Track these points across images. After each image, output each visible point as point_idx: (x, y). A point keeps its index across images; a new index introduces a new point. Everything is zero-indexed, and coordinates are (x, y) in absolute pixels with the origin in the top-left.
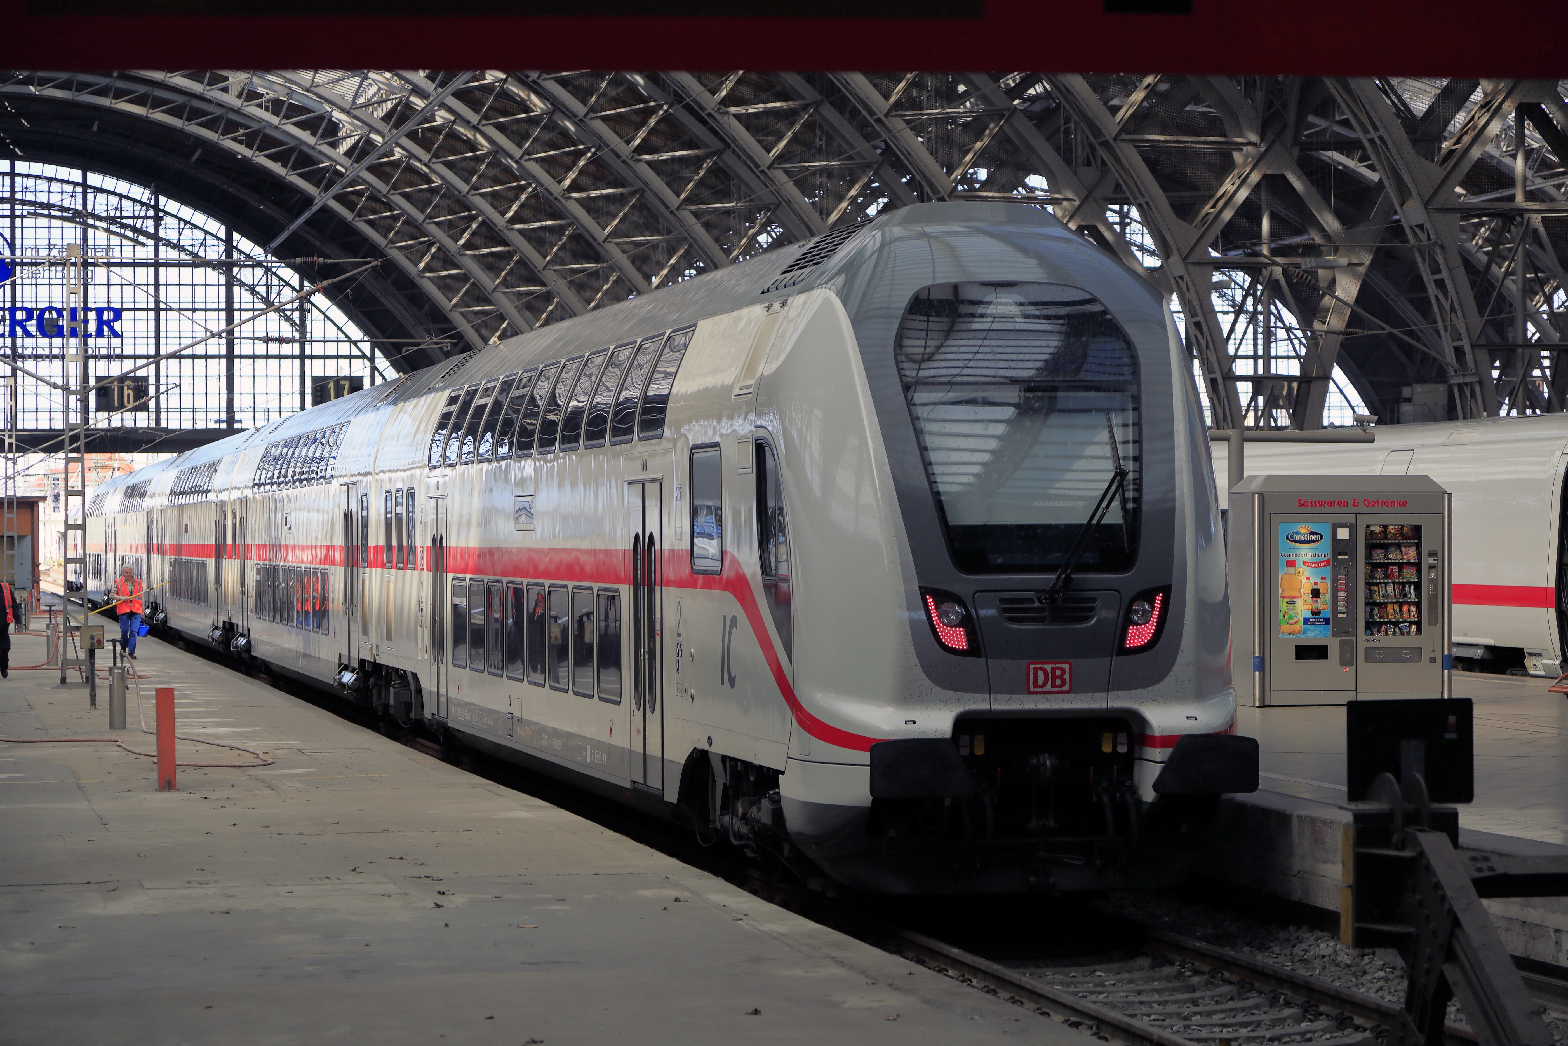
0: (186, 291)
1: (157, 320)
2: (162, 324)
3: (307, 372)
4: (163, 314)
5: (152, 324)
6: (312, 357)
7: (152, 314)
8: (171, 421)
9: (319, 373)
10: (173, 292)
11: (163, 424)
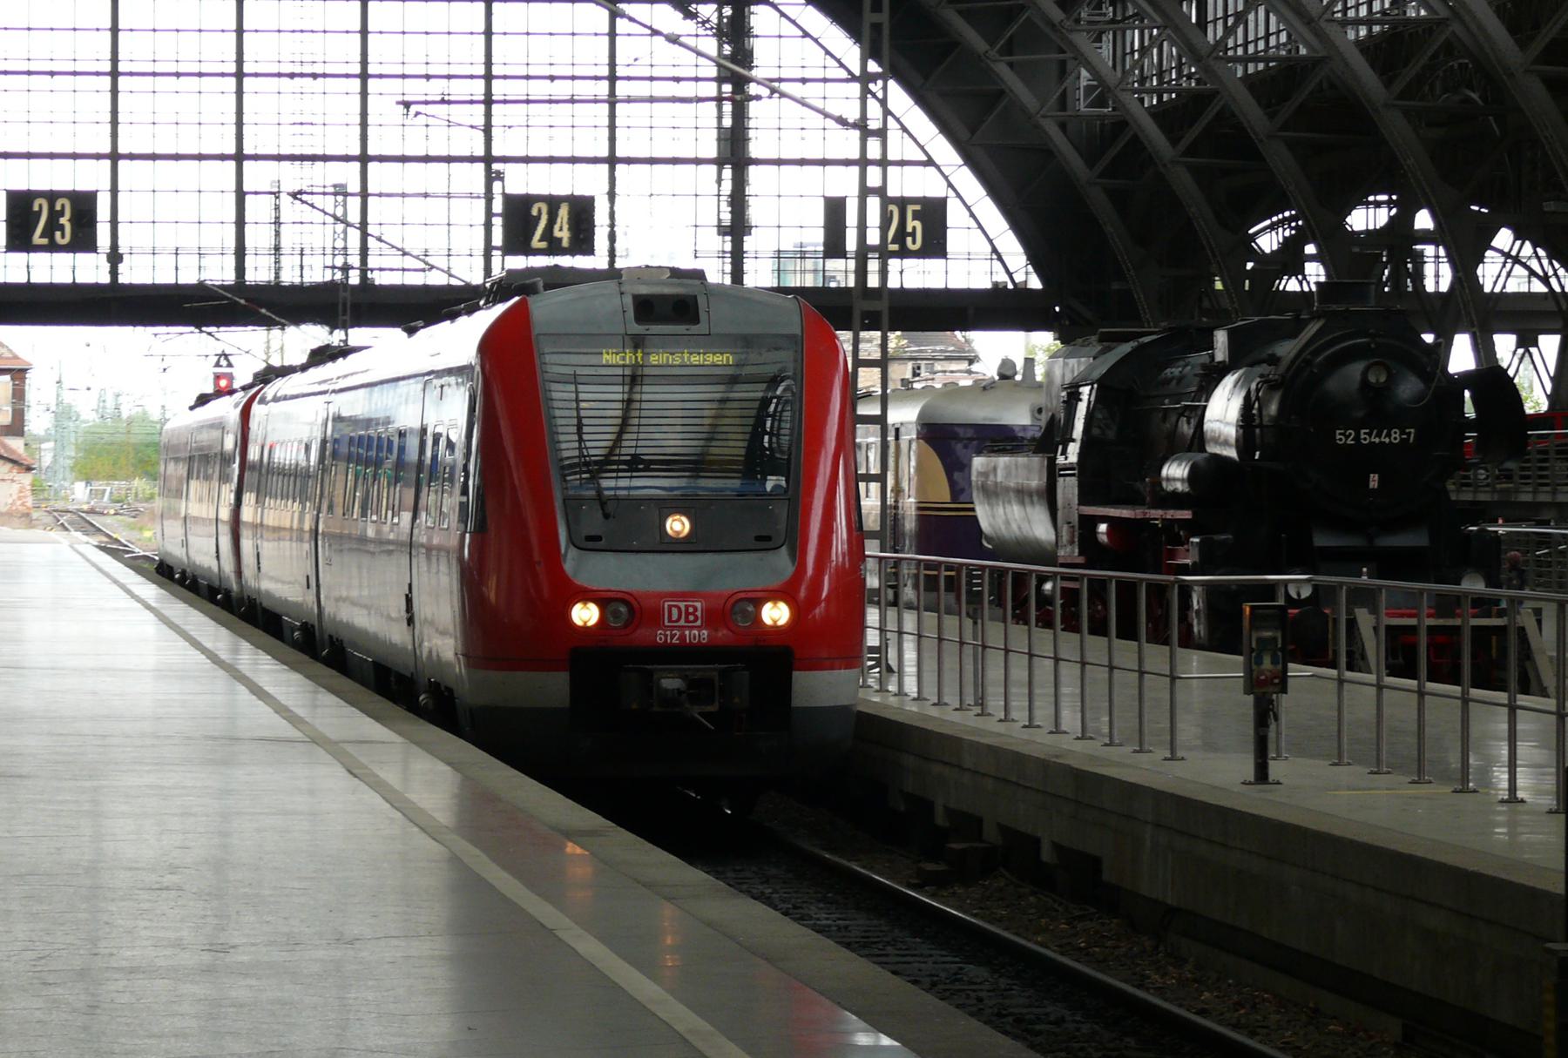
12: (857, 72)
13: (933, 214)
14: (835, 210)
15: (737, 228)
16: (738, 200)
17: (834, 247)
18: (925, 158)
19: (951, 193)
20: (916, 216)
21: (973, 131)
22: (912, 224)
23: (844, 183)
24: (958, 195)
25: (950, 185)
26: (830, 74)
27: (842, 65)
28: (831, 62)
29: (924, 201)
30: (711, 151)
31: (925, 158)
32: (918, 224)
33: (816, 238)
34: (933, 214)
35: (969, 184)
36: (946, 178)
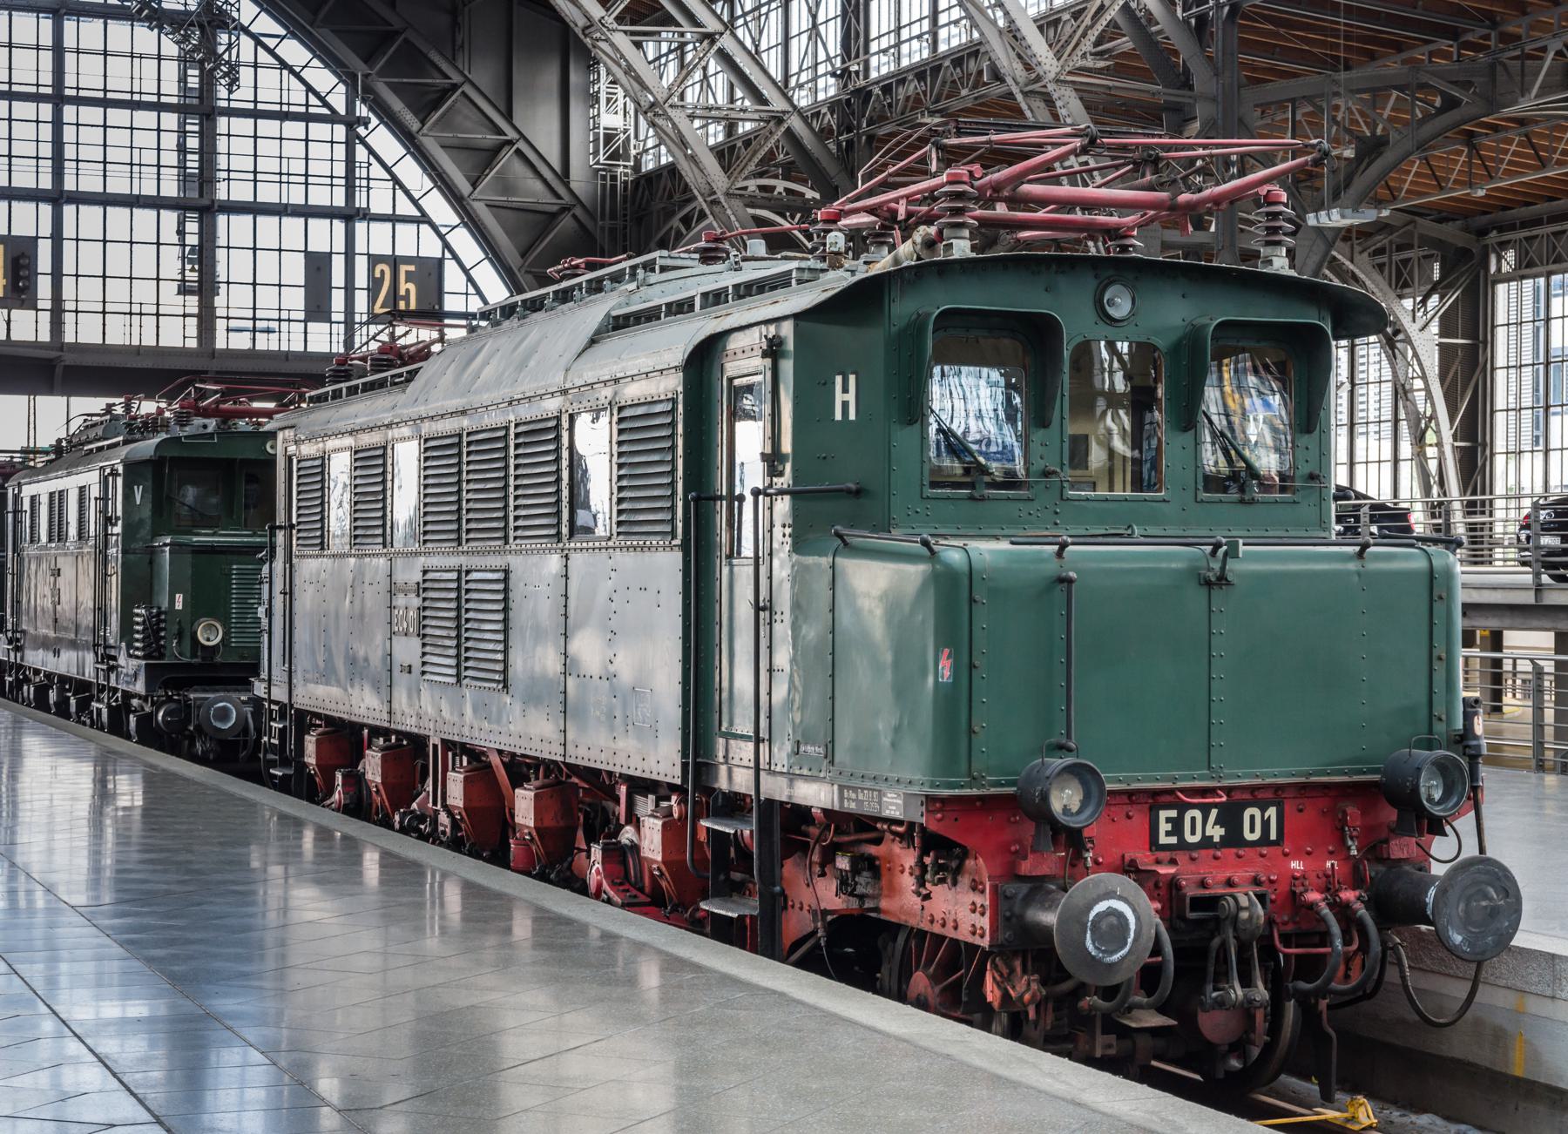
0: (118, 67)
1: (58, 123)
2: (69, 134)
3: (360, 246)
4: (69, 112)
5: (46, 132)
6: (367, 216)
7: (46, 110)
8: (84, 331)
9: (382, 247)
10: (91, 65)
11: (69, 338)
12: (342, 110)
13: (430, 273)
14: (317, 265)
15: (204, 286)
16: (204, 256)
17: (317, 309)
18: (416, 213)
19: (448, 255)
20: (410, 277)
21: (474, 185)
22: (403, 287)
23: (327, 237)
24: (455, 257)
25: (447, 246)
26: (311, 110)
27: (326, 104)
28: (313, 100)
29: (417, 260)
30: (170, 189)
31: (416, 213)
32: (412, 287)
33: (296, 300)
34: (430, 273)
35: (465, 244)
36: (442, 237)
